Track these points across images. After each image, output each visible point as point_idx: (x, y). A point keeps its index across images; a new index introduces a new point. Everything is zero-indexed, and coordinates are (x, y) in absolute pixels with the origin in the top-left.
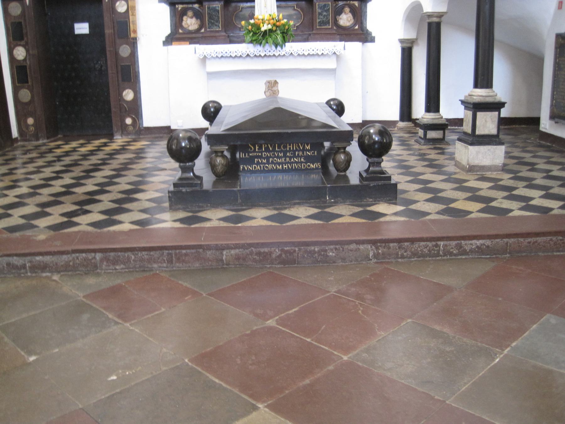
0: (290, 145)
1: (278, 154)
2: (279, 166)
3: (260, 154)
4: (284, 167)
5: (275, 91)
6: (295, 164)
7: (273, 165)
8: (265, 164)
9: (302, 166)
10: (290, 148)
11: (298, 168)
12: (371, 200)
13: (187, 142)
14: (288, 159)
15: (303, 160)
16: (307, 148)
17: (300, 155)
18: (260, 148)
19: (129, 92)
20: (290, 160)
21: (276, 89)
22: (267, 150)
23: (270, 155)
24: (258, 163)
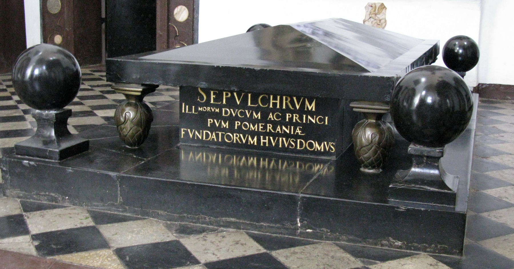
0: (275, 98)
1: (252, 115)
2: (253, 139)
3: (217, 110)
4: (262, 141)
5: (380, 20)
6: (284, 139)
7: (241, 135)
8: (224, 130)
9: (296, 143)
10: (275, 104)
11: (288, 146)
12: (399, 243)
13: (44, 68)
14: (269, 127)
15: (299, 132)
16: (310, 108)
17: (294, 121)
18: (219, 97)
19: (182, 9)
20: (274, 128)
21: (383, 17)
22: (231, 103)
23: (237, 115)
24: (213, 128)
